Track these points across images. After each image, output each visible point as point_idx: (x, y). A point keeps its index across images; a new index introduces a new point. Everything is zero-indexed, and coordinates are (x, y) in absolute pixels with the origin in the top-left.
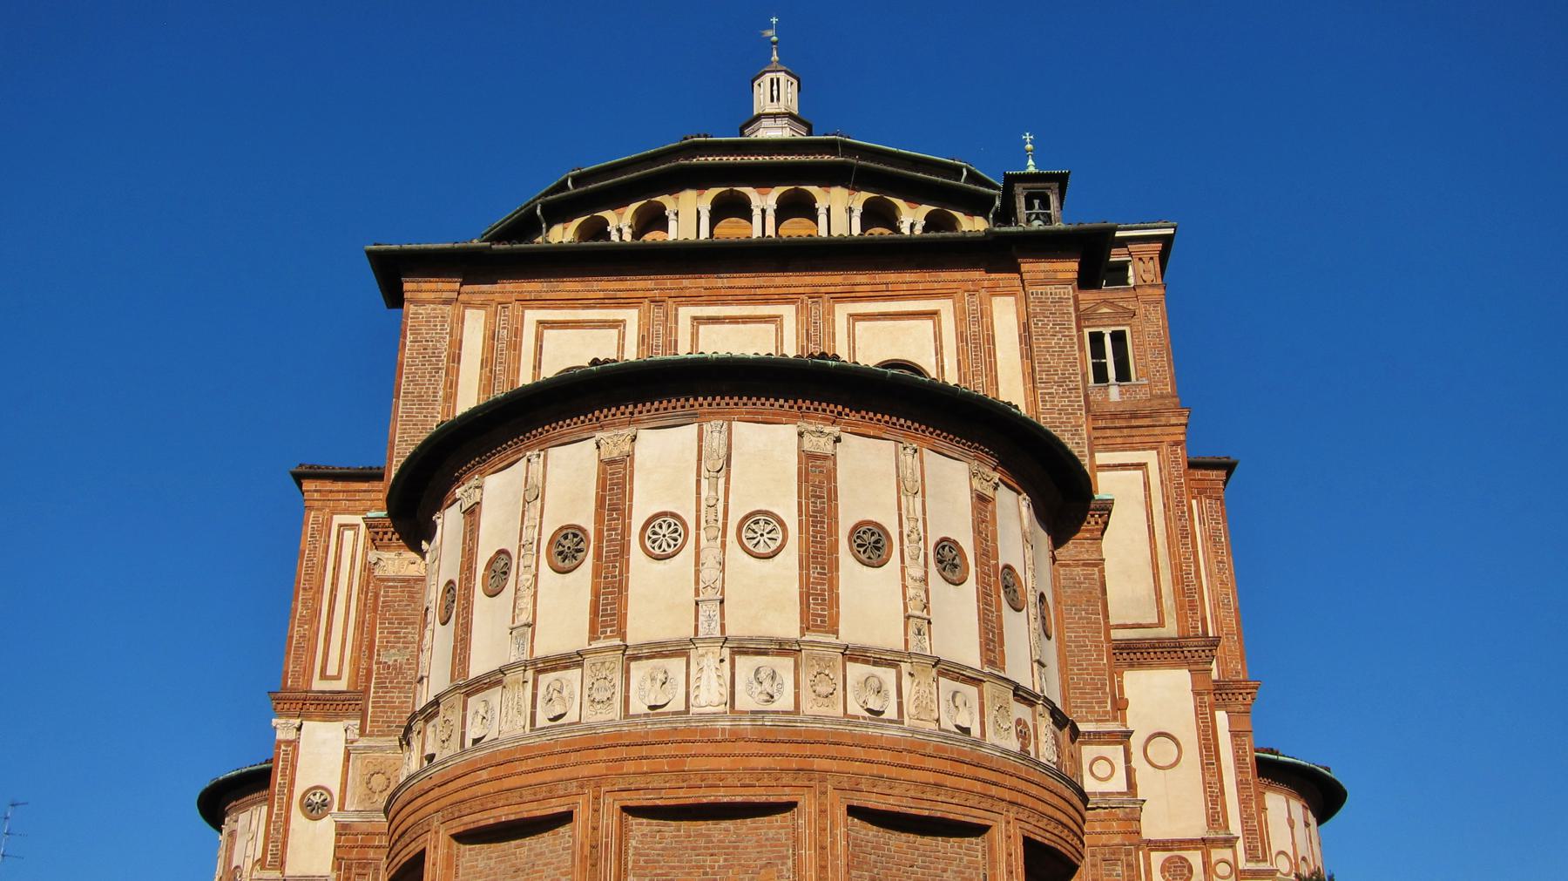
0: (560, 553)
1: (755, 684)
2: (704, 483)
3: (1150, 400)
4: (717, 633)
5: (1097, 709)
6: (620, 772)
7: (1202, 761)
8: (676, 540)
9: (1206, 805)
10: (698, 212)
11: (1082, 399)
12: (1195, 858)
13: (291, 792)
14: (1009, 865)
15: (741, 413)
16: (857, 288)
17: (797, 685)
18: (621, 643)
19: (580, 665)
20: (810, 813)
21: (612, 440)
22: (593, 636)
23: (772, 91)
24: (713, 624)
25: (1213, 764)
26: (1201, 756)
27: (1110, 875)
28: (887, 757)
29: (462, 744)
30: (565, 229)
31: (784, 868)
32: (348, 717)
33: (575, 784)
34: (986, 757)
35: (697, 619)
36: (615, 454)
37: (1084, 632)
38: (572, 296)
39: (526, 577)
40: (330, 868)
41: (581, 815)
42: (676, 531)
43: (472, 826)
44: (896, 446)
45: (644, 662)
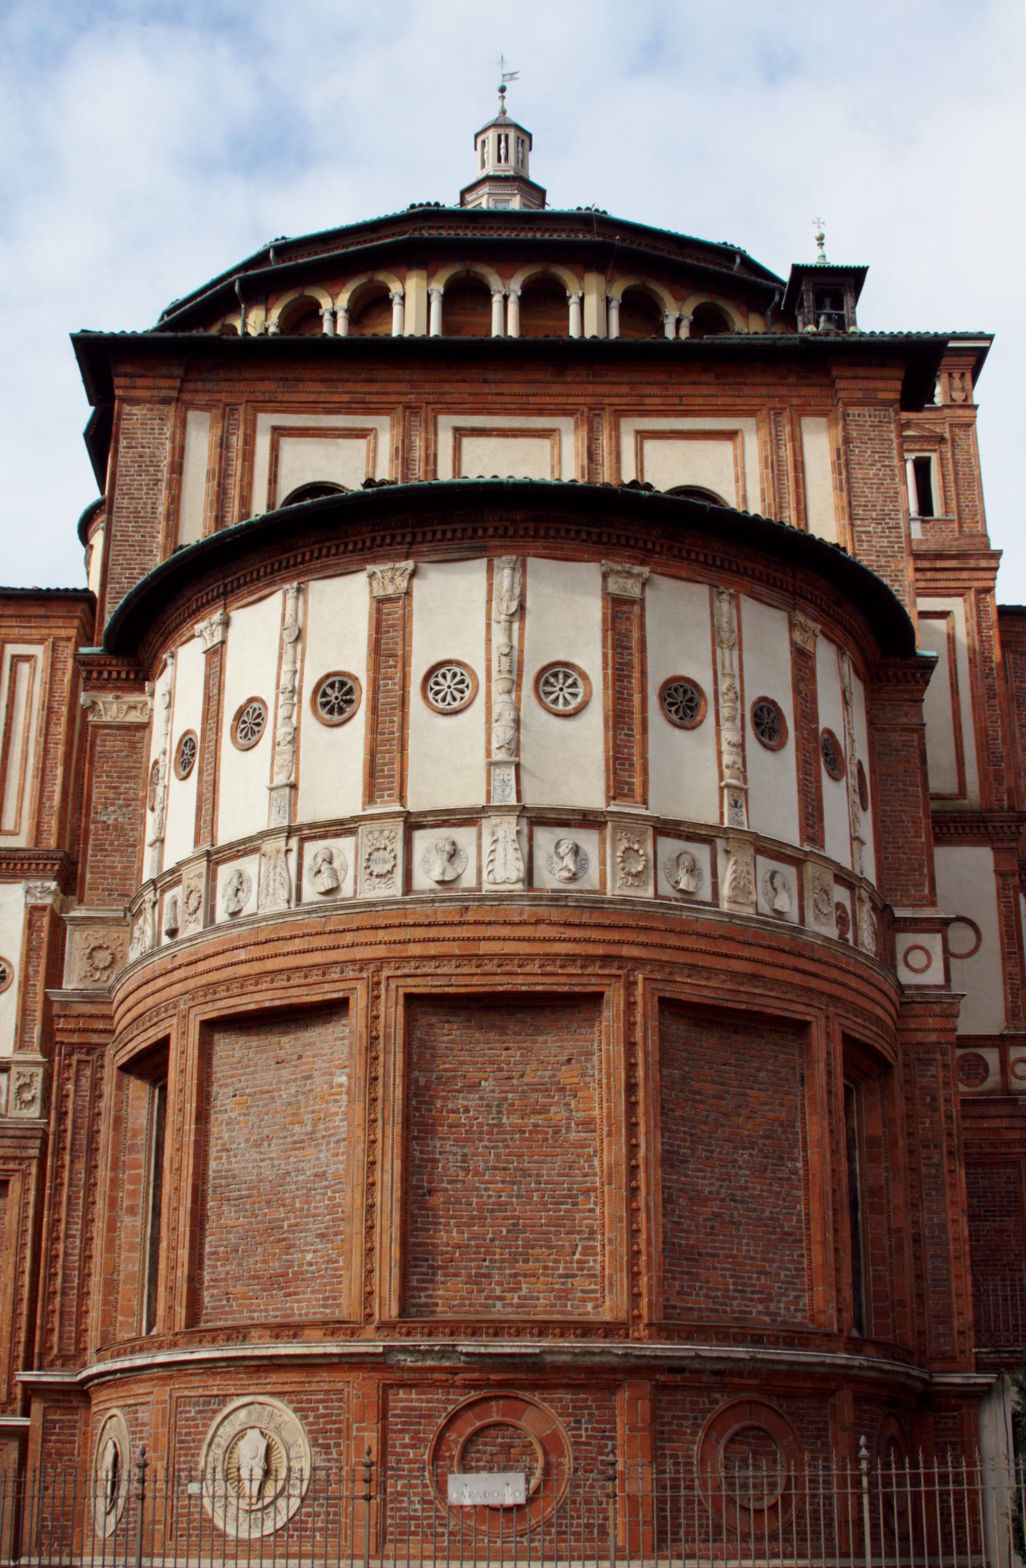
0: (324, 705)
1: (556, 859)
2: (494, 625)
3: (957, 539)
4: (513, 801)
5: (913, 892)
6: (404, 955)
7: (1003, 949)
8: (462, 692)
9: (1006, 999)
10: (429, 296)
11: (903, 539)
12: (992, 1057)
14: (828, 1064)
15: (536, 548)
16: (647, 401)
17: (603, 862)
18: (402, 809)
19: (352, 832)
20: (618, 1004)
23: (499, 149)
24: (508, 790)
25: (1015, 953)
26: (1002, 944)
27: (923, 1076)
28: (702, 945)
30: (268, 311)
31: (589, 1065)
32: (27, 878)
33: (351, 967)
34: (807, 944)
36: (390, 590)
37: (901, 805)
38: (312, 398)
39: (283, 731)
40: (11, 1049)
41: (359, 1002)
42: (462, 682)
44: (711, 591)
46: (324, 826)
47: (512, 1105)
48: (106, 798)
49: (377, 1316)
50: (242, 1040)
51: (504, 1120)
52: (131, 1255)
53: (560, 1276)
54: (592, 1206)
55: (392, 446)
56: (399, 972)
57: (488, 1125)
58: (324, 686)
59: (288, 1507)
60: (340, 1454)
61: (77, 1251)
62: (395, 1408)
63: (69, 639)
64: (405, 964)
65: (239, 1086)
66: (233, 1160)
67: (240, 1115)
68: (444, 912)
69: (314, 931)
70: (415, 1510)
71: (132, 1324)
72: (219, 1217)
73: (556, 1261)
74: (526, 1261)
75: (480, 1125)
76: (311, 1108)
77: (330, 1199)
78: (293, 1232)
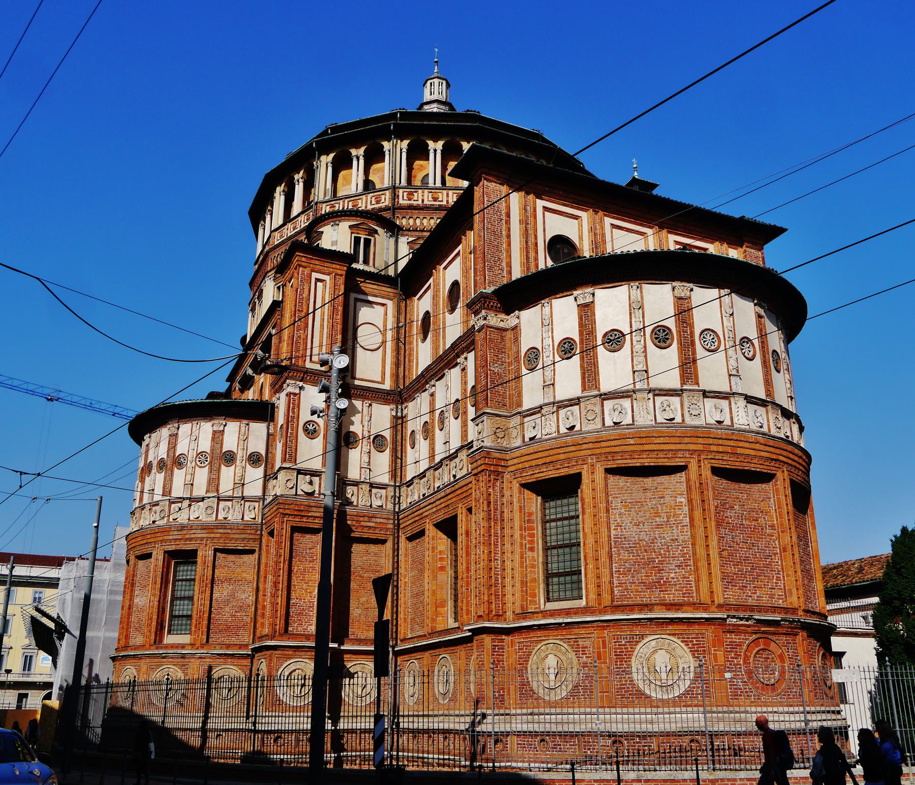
1: (755, 418)
2: (724, 317)
8: (714, 343)
21: (683, 288)
22: (683, 384)
29: (604, 424)
35: (730, 383)
36: (683, 295)
41: (693, 466)
43: (624, 465)
45: (710, 399)
46: (667, 391)
49: (716, 602)
53: (770, 589)
58: (656, 330)
59: (684, 686)
60: (705, 661)
61: (499, 566)
62: (726, 642)
63: (341, 275)
65: (623, 498)
66: (624, 531)
67: (625, 511)
69: (670, 435)
70: (740, 686)
71: (536, 601)
72: (619, 554)
73: (768, 582)
74: (758, 582)
75: (736, 524)
77: (681, 551)
78: (662, 564)
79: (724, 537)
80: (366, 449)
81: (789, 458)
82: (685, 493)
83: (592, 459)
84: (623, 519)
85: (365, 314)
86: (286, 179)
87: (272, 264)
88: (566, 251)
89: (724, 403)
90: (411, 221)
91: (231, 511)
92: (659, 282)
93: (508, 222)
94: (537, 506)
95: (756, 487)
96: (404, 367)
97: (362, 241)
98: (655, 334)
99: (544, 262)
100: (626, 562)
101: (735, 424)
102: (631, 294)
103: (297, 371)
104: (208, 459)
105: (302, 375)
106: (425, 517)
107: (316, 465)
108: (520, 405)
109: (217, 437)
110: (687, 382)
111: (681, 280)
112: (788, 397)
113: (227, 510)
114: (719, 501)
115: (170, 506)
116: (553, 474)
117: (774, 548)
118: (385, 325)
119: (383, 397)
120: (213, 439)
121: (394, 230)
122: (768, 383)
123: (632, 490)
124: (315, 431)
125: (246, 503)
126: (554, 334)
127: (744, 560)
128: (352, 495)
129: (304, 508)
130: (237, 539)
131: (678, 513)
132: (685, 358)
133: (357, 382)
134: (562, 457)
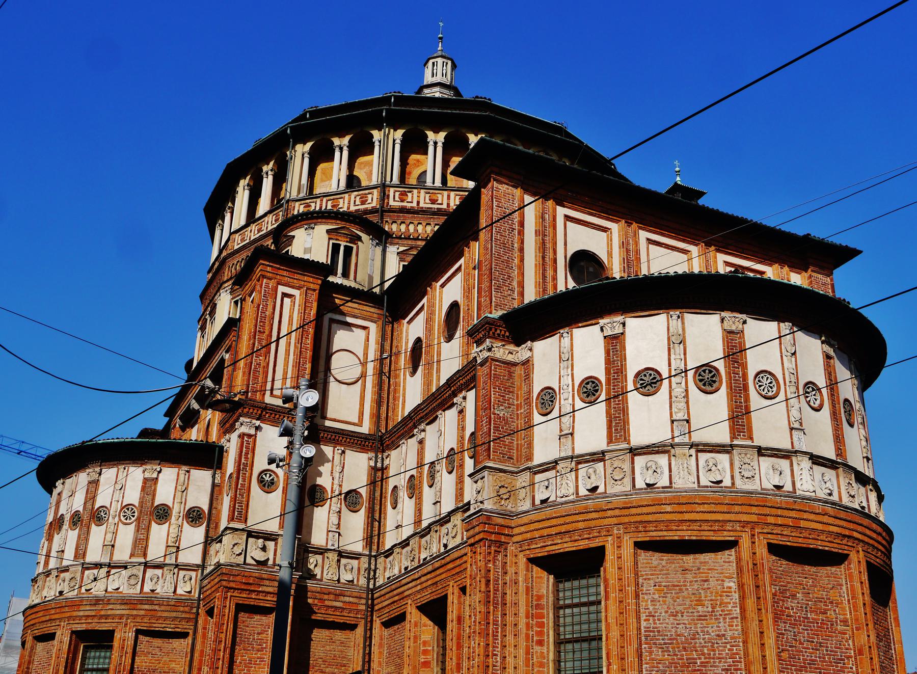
1: (823, 483)
2: (784, 357)
8: (771, 388)
13: (252, 470)
19: (727, 452)
21: (733, 320)
29: (634, 486)
30: (395, 130)
33: (738, 525)
36: (734, 328)
40: (278, 527)
41: (745, 542)
43: (658, 539)
45: (766, 458)
46: (713, 446)
47: (811, 608)
48: (499, 401)
50: (657, 555)
51: (809, 616)
52: (541, 669)
54: (851, 666)
55: (619, 241)
56: (765, 531)
57: (803, 617)
58: (700, 370)
61: (499, 664)
63: (314, 290)
64: (766, 527)
65: (657, 580)
66: (658, 622)
67: (659, 597)
68: (785, 502)
69: (717, 502)
72: (651, 653)
75: (799, 617)
76: (709, 598)
77: (729, 650)
78: (705, 666)
79: (783, 634)
80: (335, 508)
81: (865, 535)
82: (735, 576)
83: (619, 529)
84: (657, 607)
85: (341, 338)
86: (252, 171)
87: (230, 274)
88: (591, 269)
89: (784, 464)
90: (403, 227)
91: (161, 581)
92: (705, 312)
93: (521, 233)
94: (548, 587)
95: (824, 571)
96: (388, 406)
97: (342, 249)
98: (700, 375)
99: (565, 282)
100: (659, 663)
101: (797, 491)
102: (671, 325)
103: (254, 406)
104: (136, 514)
105: (259, 412)
106: (406, 597)
107: (273, 526)
108: (530, 458)
109: (149, 486)
110: (739, 435)
111: (732, 310)
112: (864, 458)
113: (155, 580)
114: (778, 588)
115: (83, 573)
116: (568, 546)
117: (847, 649)
118: (366, 354)
119: (359, 442)
120: (143, 488)
121: (382, 238)
122: (839, 439)
123: (668, 570)
124: (273, 483)
125: (181, 572)
126: (574, 372)
127: (809, 664)
128: (316, 566)
129: (254, 580)
130: (166, 618)
131: (726, 601)
132: (736, 405)
133: (328, 423)
134: (581, 525)
